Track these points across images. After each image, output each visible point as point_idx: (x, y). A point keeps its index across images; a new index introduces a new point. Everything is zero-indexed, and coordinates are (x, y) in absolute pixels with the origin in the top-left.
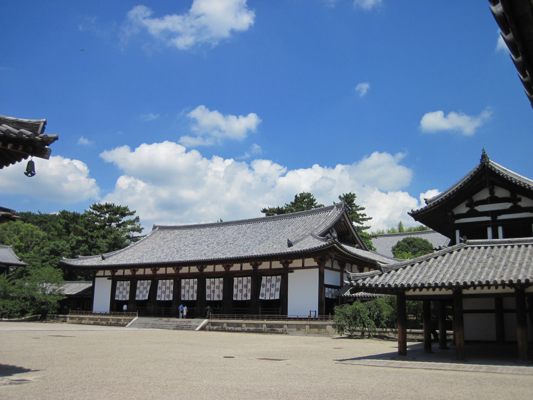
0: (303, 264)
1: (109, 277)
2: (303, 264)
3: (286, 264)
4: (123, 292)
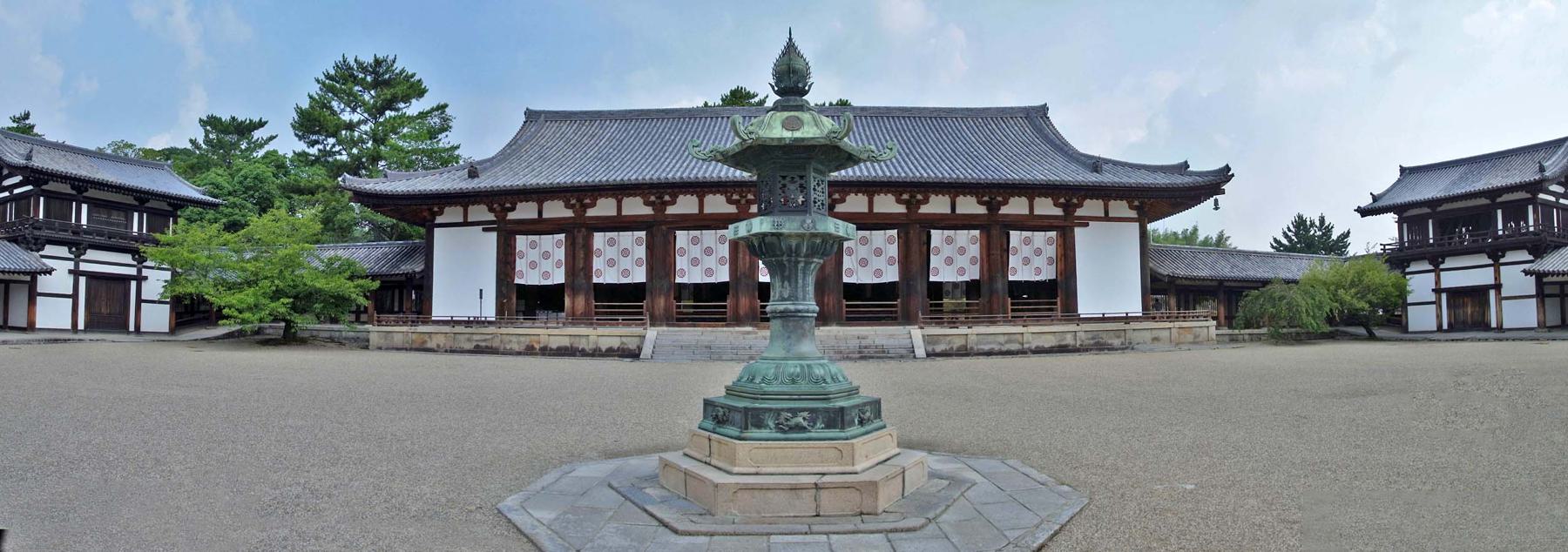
0: (1106, 212)
1: (487, 227)
2: (1106, 212)
3: (1069, 208)
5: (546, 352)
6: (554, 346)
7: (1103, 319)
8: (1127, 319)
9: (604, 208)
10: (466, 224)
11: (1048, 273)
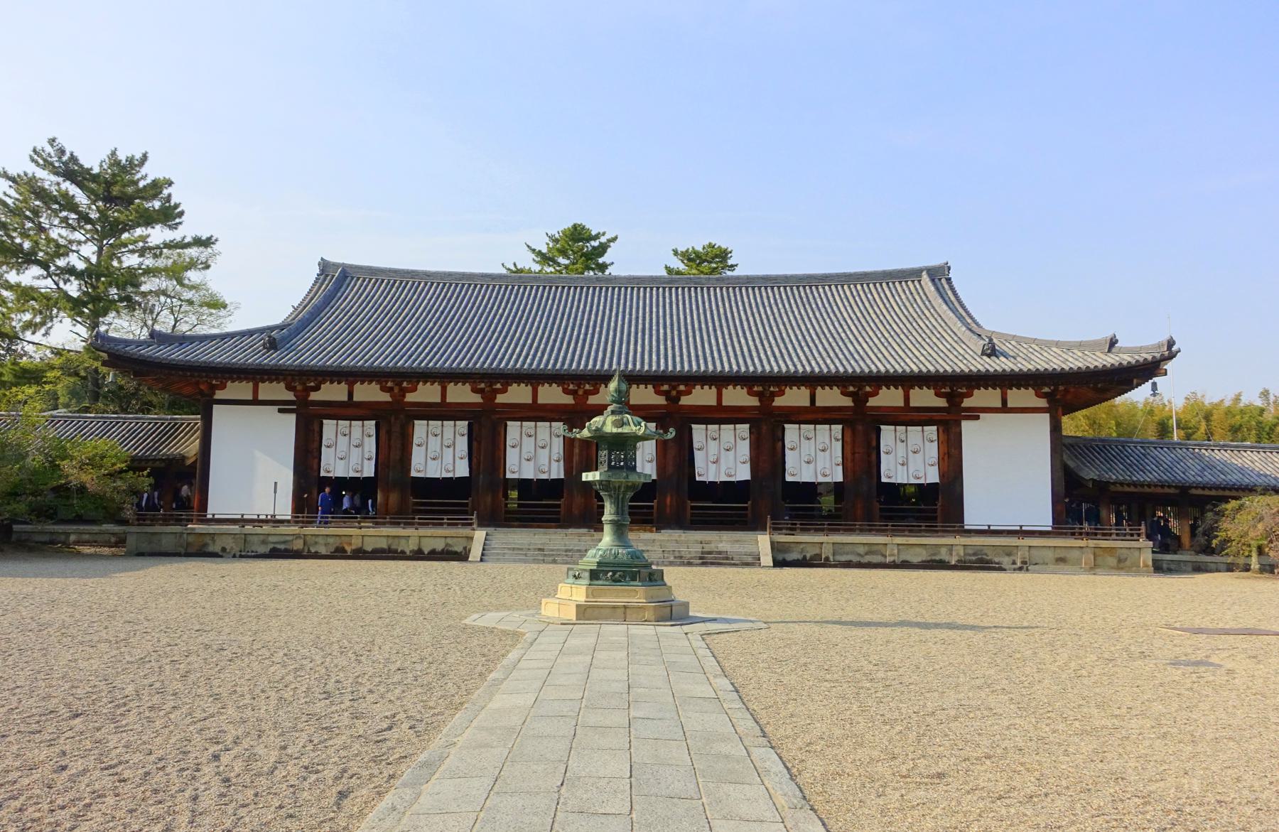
0: (1004, 401)
4: (349, 452)
5: (360, 554)
6: (369, 549)
7: (989, 532)
8: (1022, 533)
9: (427, 393)
10: (255, 402)
11: (933, 476)
